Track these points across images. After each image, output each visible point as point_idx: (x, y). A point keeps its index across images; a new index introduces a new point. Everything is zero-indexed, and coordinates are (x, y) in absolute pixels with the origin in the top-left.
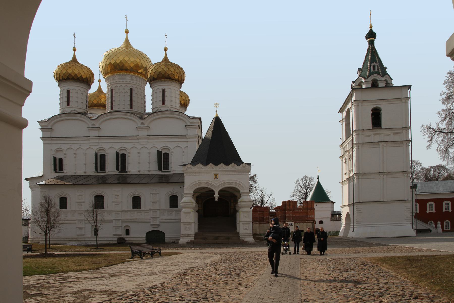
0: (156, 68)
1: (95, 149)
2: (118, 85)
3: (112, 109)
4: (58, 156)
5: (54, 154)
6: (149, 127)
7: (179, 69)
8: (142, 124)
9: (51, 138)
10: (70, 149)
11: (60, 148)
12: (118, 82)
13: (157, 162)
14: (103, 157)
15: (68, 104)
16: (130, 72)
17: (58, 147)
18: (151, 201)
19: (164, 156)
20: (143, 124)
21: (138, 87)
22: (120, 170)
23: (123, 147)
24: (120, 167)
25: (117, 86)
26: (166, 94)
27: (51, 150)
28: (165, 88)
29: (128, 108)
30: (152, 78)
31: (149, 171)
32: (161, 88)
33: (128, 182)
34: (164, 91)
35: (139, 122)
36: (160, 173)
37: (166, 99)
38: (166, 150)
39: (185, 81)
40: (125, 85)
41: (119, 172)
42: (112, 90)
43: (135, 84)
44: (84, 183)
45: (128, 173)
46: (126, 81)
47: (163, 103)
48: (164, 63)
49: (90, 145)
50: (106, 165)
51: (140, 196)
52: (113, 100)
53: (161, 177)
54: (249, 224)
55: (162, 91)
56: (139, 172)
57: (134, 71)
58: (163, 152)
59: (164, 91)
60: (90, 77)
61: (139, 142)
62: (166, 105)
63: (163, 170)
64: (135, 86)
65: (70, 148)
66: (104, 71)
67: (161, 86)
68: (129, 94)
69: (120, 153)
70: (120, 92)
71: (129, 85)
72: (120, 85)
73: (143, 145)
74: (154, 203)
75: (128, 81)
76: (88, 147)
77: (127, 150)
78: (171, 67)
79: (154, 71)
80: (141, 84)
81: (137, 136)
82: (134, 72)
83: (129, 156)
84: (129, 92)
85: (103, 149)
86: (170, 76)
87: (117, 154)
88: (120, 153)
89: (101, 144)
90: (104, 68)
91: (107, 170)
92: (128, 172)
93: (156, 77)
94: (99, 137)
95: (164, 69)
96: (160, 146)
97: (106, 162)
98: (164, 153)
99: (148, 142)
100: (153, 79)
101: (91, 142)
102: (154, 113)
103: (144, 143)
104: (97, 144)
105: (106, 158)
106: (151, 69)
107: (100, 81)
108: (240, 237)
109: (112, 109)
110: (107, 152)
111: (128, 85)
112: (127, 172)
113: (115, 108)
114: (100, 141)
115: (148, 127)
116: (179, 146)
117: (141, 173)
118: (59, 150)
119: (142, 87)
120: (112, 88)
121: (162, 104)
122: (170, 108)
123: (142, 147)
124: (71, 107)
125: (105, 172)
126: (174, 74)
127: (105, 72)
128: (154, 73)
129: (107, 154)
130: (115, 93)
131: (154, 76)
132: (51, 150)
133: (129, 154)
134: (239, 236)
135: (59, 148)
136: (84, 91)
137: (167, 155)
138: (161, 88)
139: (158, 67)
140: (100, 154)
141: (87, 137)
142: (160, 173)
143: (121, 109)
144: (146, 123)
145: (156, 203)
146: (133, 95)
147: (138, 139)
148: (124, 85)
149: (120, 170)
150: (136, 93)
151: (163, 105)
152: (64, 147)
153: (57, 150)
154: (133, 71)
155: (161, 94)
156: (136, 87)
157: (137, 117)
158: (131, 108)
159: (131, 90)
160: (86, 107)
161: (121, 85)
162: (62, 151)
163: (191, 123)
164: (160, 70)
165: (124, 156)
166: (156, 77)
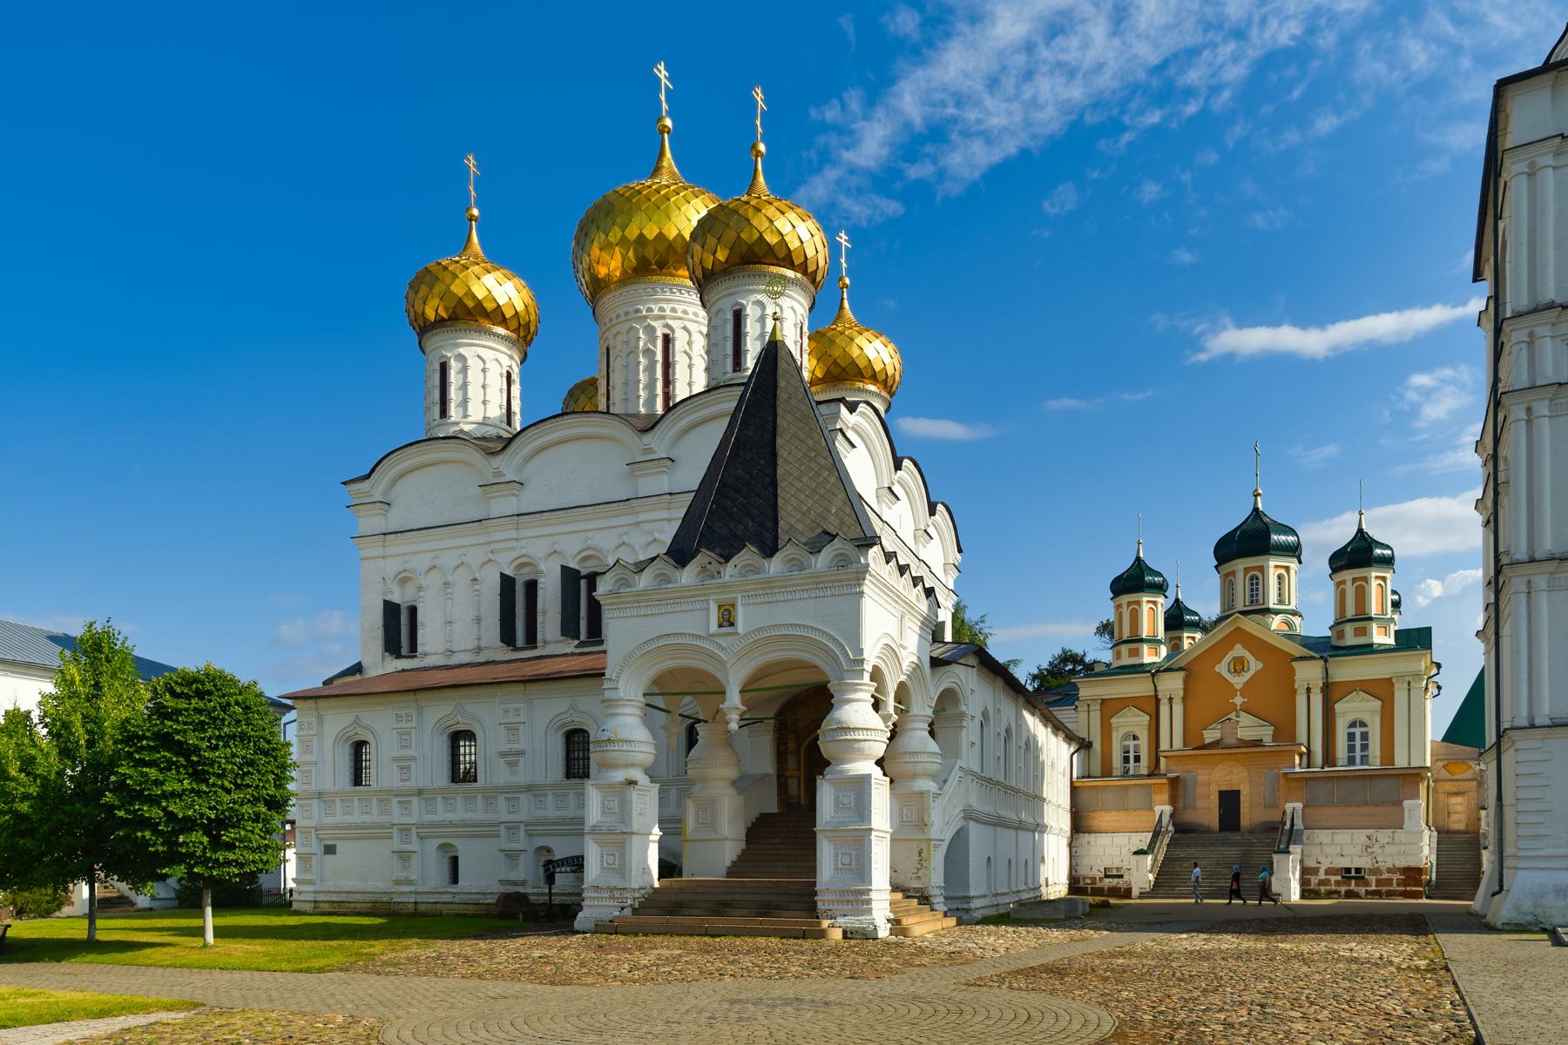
14: (532, 587)
22: (583, 637)
27: (384, 578)
41: (582, 644)
49: (492, 552)
61: (637, 524)
81: (631, 501)
85: (531, 561)
87: (570, 577)
89: (523, 543)
99: (668, 520)
104: (515, 544)
115: (669, 463)
125: (536, 647)
140: (522, 582)
149: (583, 637)
153: (400, 577)
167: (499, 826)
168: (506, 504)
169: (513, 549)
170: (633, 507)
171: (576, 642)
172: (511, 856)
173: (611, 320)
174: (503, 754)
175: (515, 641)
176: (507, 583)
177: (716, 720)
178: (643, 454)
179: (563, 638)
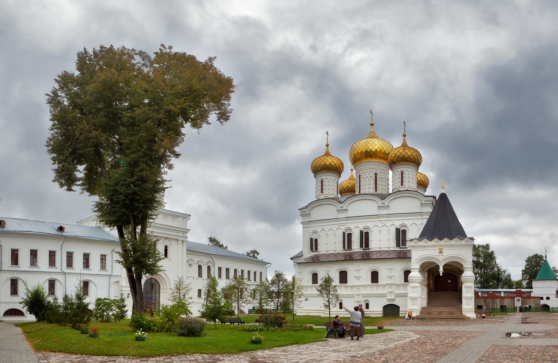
0: (395, 152)
1: (343, 229)
2: (365, 171)
3: (360, 193)
7: (416, 152)
8: (383, 204)
10: (357, 227)
14: (350, 235)
15: (322, 192)
18: (387, 276)
19: (402, 233)
20: (384, 204)
21: (382, 171)
22: (364, 248)
24: (364, 244)
25: (363, 172)
26: (404, 176)
29: (372, 191)
30: (392, 162)
32: (400, 170)
33: (372, 258)
34: (402, 173)
35: (380, 202)
36: (398, 249)
37: (404, 180)
38: (403, 227)
39: (422, 163)
40: (371, 170)
42: (360, 176)
43: (379, 169)
44: (331, 260)
45: (371, 250)
46: (372, 167)
47: (402, 184)
48: (402, 148)
52: (361, 185)
53: (400, 252)
54: (472, 299)
55: (401, 173)
56: (380, 248)
58: (401, 230)
59: (402, 173)
60: (339, 166)
61: (380, 221)
63: (401, 247)
67: (399, 169)
71: (374, 171)
72: (366, 170)
73: (384, 223)
74: (390, 278)
75: (373, 166)
76: (338, 228)
77: (369, 228)
78: (408, 151)
79: (393, 156)
84: (374, 176)
85: (350, 228)
86: (408, 159)
87: (361, 232)
89: (348, 224)
90: (352, 157)
91: (353, 248)
95: (402, 153)
96: (398, 223)
97: (352, 240)
98: (402, 230)
99: (388, 220)
100: (393, 162)
101: (340, 222)
102: (393, 193)
106: (391, 154)
107: (352, 170)
109: (360, 193)
110: (353, 231)
111: (373, 170)
112: (369, 249)
113: (362, 192)
116: (415, 223)
117: (382, 249)
119: (385, 171)
120: (359, 174)
122: (407, 188)
123: (383, 225)
124: (324, 194)
129: (353, 233)
131: (394, 161)
133: (372, 232)
136: (335, 179)
137: (404, 232)
138: (400, 170)
141: (337, 218)
142: (398, 249)
143: (367, 192)
144: (386, 202)
146: (378, 179)
148: (369, 171)
149: (364, 248)
150: (380, 177)
152: (319, 229)
155: (400, 176)
157: (378, 198)
158: (376, 190)
159: (376, 174)
160: (337, 193)
162: (316, 232)
163: (425, 201)
164: (398, 154)
165: (367, 234)
166: (395, 161)
169: (345, 225)
171: (362, 249)
173: (359, 170)
174: (355, 277)
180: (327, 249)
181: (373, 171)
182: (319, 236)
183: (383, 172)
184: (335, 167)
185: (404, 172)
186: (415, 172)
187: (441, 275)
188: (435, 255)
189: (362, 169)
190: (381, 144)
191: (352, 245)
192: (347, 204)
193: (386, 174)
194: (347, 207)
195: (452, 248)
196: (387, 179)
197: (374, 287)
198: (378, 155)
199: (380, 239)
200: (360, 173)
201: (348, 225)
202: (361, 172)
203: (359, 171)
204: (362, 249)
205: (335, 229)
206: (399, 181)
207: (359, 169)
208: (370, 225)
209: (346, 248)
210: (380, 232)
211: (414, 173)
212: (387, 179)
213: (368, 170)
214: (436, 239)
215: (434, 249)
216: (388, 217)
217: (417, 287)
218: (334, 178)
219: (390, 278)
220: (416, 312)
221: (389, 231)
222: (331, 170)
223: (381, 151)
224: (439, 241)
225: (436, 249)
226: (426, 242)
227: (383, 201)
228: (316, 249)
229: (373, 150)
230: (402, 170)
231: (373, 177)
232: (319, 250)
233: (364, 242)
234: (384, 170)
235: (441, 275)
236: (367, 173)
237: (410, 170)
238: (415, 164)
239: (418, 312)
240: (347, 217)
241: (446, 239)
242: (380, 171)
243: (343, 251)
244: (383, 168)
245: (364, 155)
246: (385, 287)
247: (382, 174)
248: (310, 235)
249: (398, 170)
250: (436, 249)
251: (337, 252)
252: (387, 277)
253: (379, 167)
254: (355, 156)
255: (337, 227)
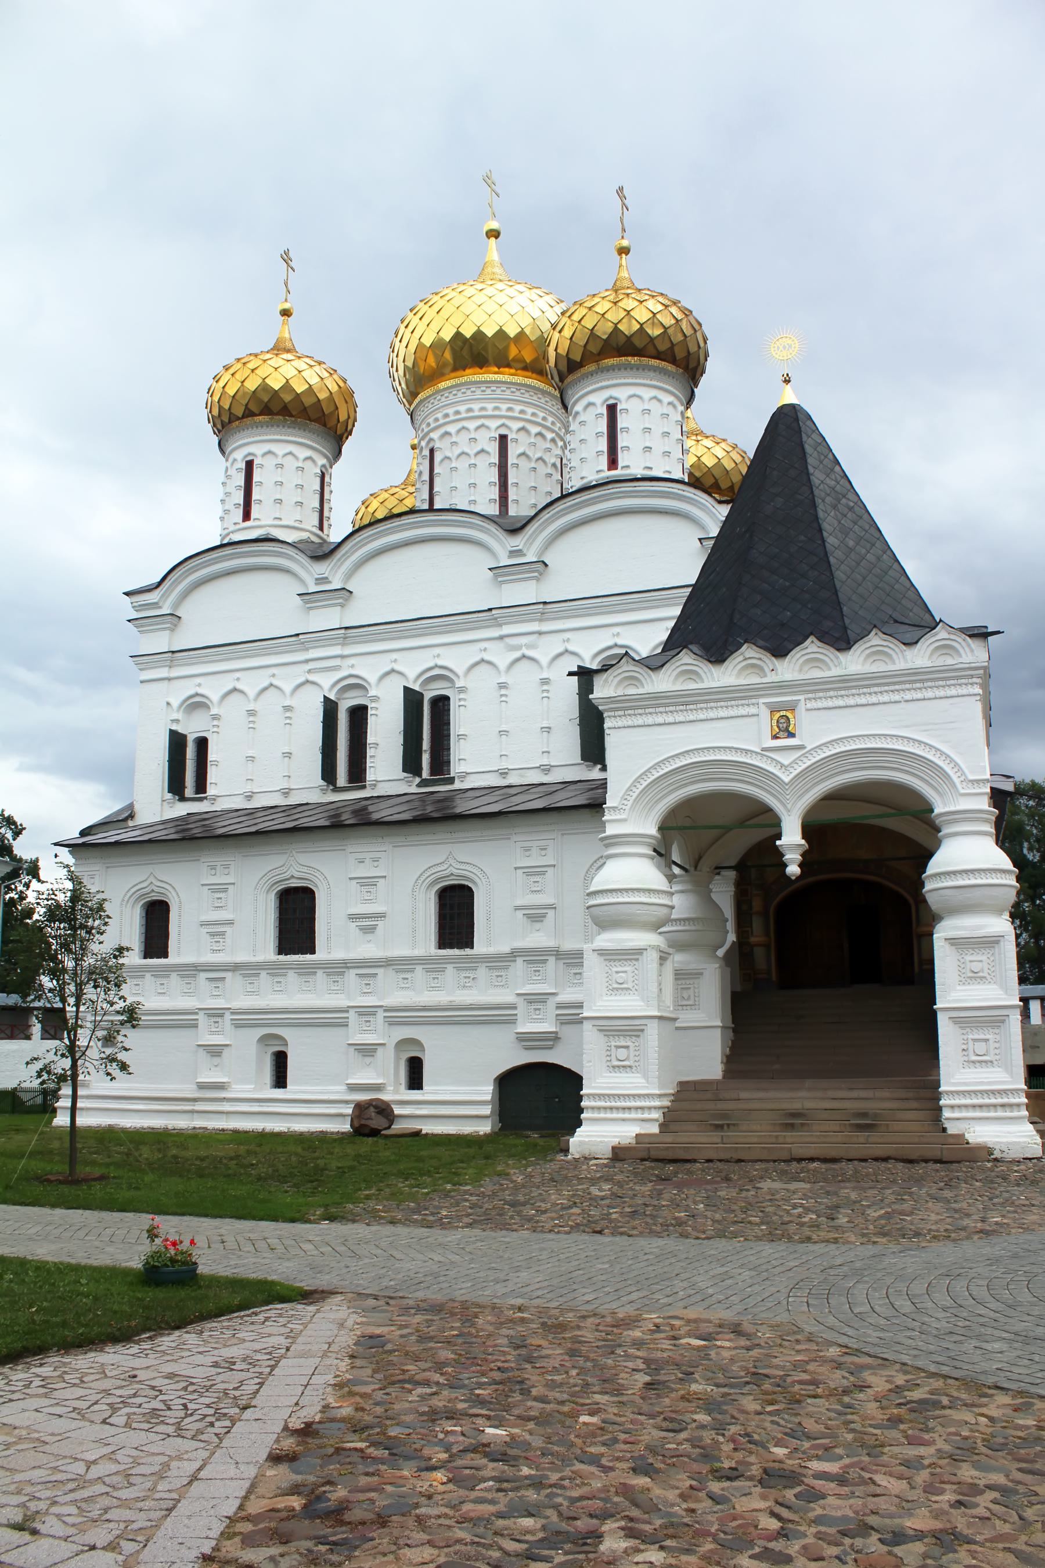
1: (327, 684)
2: (452, 429)
4: (192, 728)
5: (177, 721)
6: (546, 565)
8: (514, 553)
9: (170, 654)
11: (202, 696)
12: (452, 418)
13: (577, 721)
14: (359, 716)
16: (496, 369)
17: (192, 692)
18: (517, 908)
21: (529, 426)
22: (425, 774)
23: (436, 666)
26: (622, 422)
28: (616, 399)
30: (563, 366)
31: (546, 769)
32: (599, 399)
34: (612, 410)
37: (622, 441)
39: (710, 365)
40: (479, 422)
41: (424, 783)
42: (432, 451)
45: (457, 785)
49: (309, 671)
50: (370, 752)
51: (466, 883)
55: (605, 411)
56: (504, 774)
57: (512, 364)
59: (612, 410)
61: (501, 638)
62: (623, 467)
64: (515, 425)
65: (235, 690)
66: (404, 386)
68: (495, 459)
69: (428, 696)
70: (459, 455)
71: (493, 424)
72: (459, 425)
73: (518, 648)
74: (535, 916)
75: (490, 406)
76: (302, 679)
78: (636, 303)
80: (542, 415)
82: (513, 371)
83: (462, 703)
84: (494, 448)
86: (638, 343)
87: (412, 700)
88: (428, 696)
91: (370, 776)
92: (457, 781)
93: (578, 360)
94: (343, 631)
99: (540, 633)
103: (524, 640)
104: (337, 662)
105: (371, 720)
108: (946, 1114)
110: (372, 692)
111: (487, 422)
112: (451, 781)
114: (347, 651)
115: (540, 566)
117: (513, 779)
118: (196, 704)
120: (431, 446)
121: (605, 467)
123: (517, 660)
125: (364, 787)
126: (650, 332)
127: (408, 387)
128: (571, 339)
130: (442, 461)
131: (571, 356)
132: (168, 704)
133: (462, 696)
134: (940, 1109)
135: (197, 694)
138: (599, 399)
139: (585, 311)
141: (297, 635)
145: (544, 916)
146: (511, 459)
147: (500, 625)
148: (472, 425)
149: (425, 774)
150: (523, 454)
151: (609, 469)
152: (213, 690)
153: (188, 702)
154: (509, 366)
155: (603, 426)
156: (523, 429)
159: (503, 439)
161: (464, 428)
165: (441, 704)
167: (347, 1011)
168: (329, 618)
170: (496, 619)
171: (418, 780)
172: (367, 1051)
174: (353, 917)
175: (336, 779)
176: (330, 709)
177: (699, 868)
178: (509, 557)
179: (406, 775)
180: (249, 788)
181: (488, 428)
182: (215, 723)
183: (535, 430)
184: (308, 401)
185: (619, 407)
186: (675, 407)
187: (793, 870)
188: (747, 751)
189: (441, 421)
190: (525, 302)
191: (368, 764)
192: (348, 564)
193: (553, 440)
194: (349, 575)
195: (851, 701)
196: (554, 465)
197: (450, 968)
198: (513, 352)
199: (504, 727)
200: (431, 440)
201: (353, 666)
202: (434, 435)
203: (428, 433)
204: (418, 780)
205: (288, 688)
206: (600, 449)
207: (431, 420)
208: (456, 660)
209: (342, 779)
210: (503, 692)
211: (669, 410)
212: (554, 465)
213: (466, 424)
214: (749, 651)
215: (742, 711)
216: (542, 618)
217: (639, 951)
218: (303, 453)
219: (535, 916)
220: (639, 1115)
221: (545, 687)
222: (291, 416)
223: (522, 334)
224: (769, 661)
225: (753, 710)
226: (690, 674)
227: (517, 542)
228: (201, 785)
229: (489, 332)
230: (611, 397)
231: (488, 453)
232: (211, 791)
233: (426, 745)
234: (539, 420)
235: (793, 870)
236: (464, 436)
237: (647, 393)
238: (670, 367)
239: (646, 1116)
240: (346, 628)
241: (812, 646)
242: (520, 424)
243: (324, 791)
244: (534, 414)
245: (448, 355)
246: (506, 968)
247: (532, 440)
248: (175, 716)
249: (591, 398)
250: (753, 710)
251: (293, 800)
252: (520, 914)
253: (518, 408)
254: (410, 364)
255: (299, 674)
